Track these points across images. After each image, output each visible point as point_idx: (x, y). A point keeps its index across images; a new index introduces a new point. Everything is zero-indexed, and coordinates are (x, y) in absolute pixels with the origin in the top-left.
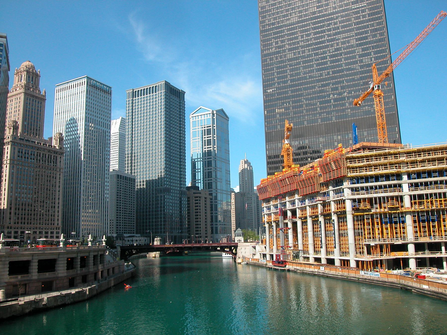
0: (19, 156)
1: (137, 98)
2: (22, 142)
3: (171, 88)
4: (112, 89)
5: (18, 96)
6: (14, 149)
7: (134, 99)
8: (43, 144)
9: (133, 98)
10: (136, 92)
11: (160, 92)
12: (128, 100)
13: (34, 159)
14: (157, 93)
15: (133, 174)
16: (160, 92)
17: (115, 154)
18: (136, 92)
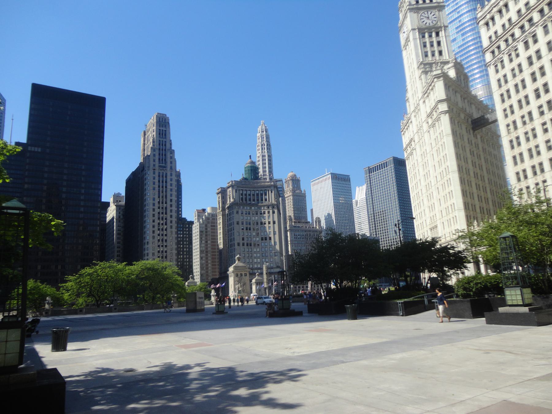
0: (295, 238)
1: (373, 173)
2: (295, 228)
3: (399, 161)
4: (350, 177)
5: (289, 198)
6: (292, 234)
7: (371, 174)
8: (309, 227)
9: (370, 174)
10: (371, 168)
11: (390, 166)
12: (366, 176)
13: (304, 238)
14: (388, 168)
15: (378, 236)
16: (390, 166)
17: (365, 216)
18: (371, 168)
